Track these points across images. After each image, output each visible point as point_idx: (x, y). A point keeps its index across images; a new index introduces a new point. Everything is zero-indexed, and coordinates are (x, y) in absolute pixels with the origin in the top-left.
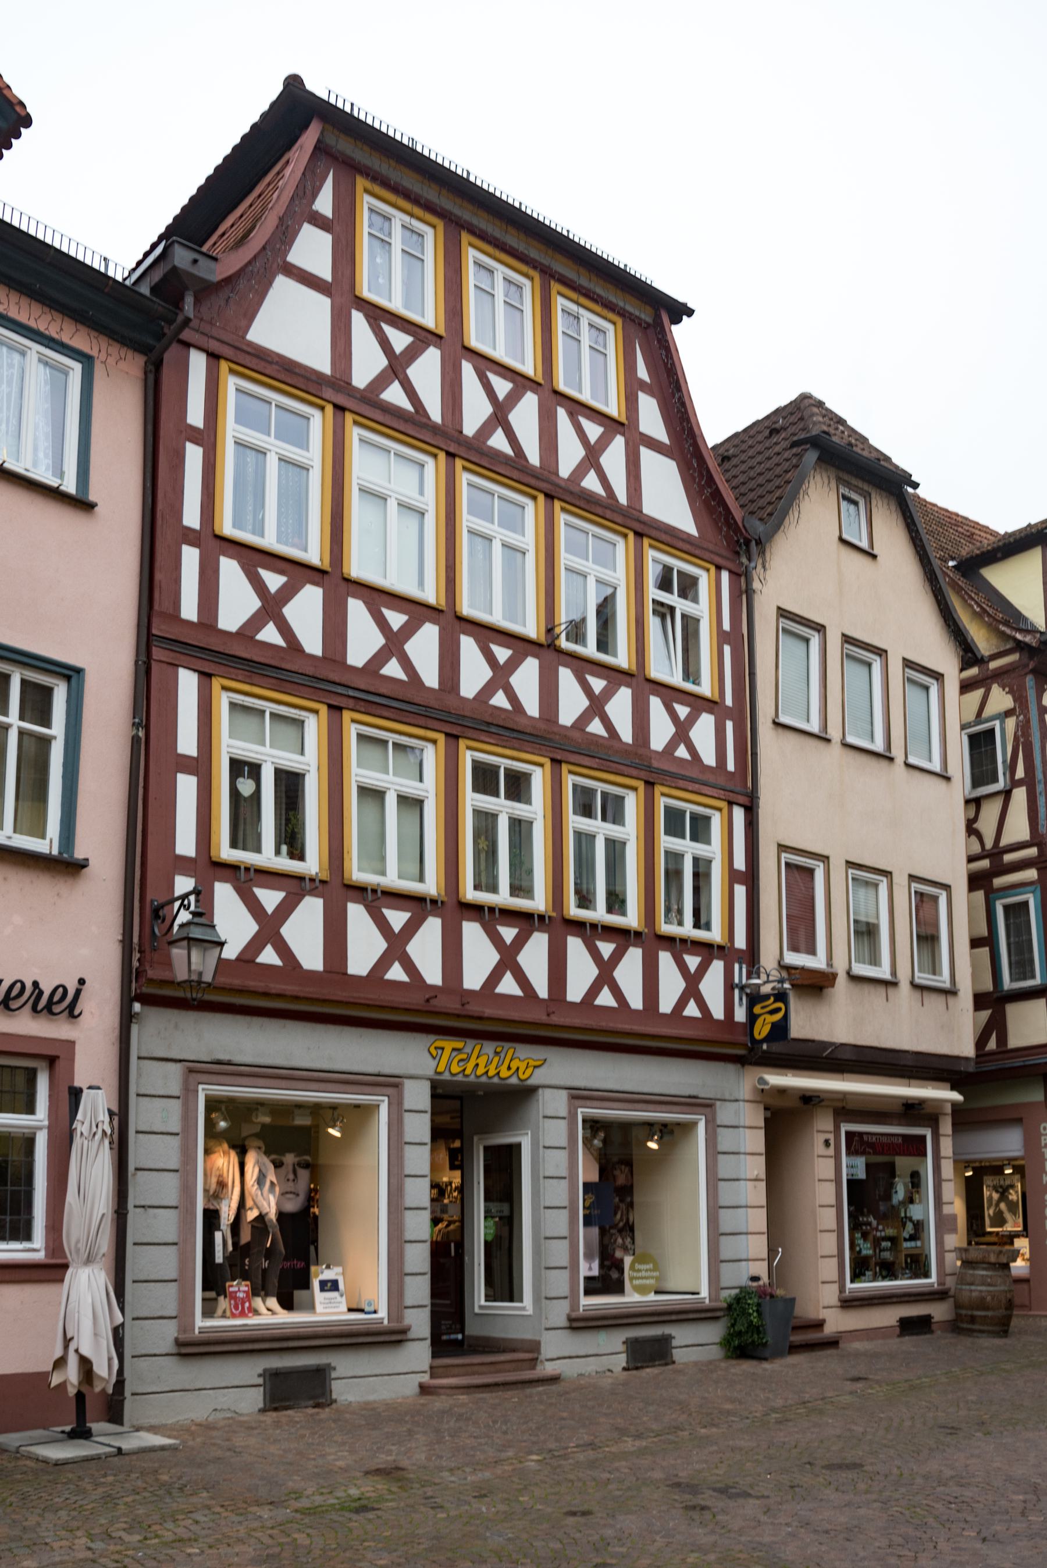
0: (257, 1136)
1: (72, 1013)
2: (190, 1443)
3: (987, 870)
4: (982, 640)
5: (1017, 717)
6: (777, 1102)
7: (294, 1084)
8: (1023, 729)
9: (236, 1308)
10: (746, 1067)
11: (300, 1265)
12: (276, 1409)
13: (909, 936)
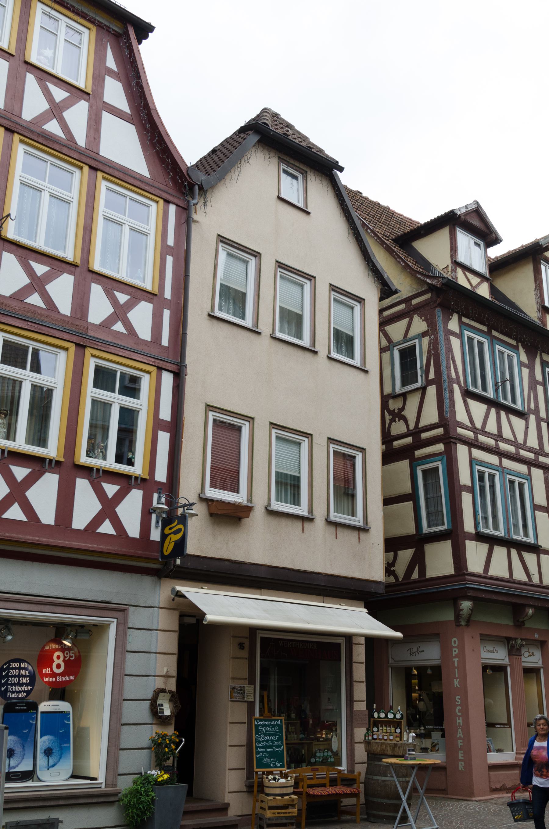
3: (410, 444)
5: (430, 337)
10: (163, 579)
13: (326, 483)
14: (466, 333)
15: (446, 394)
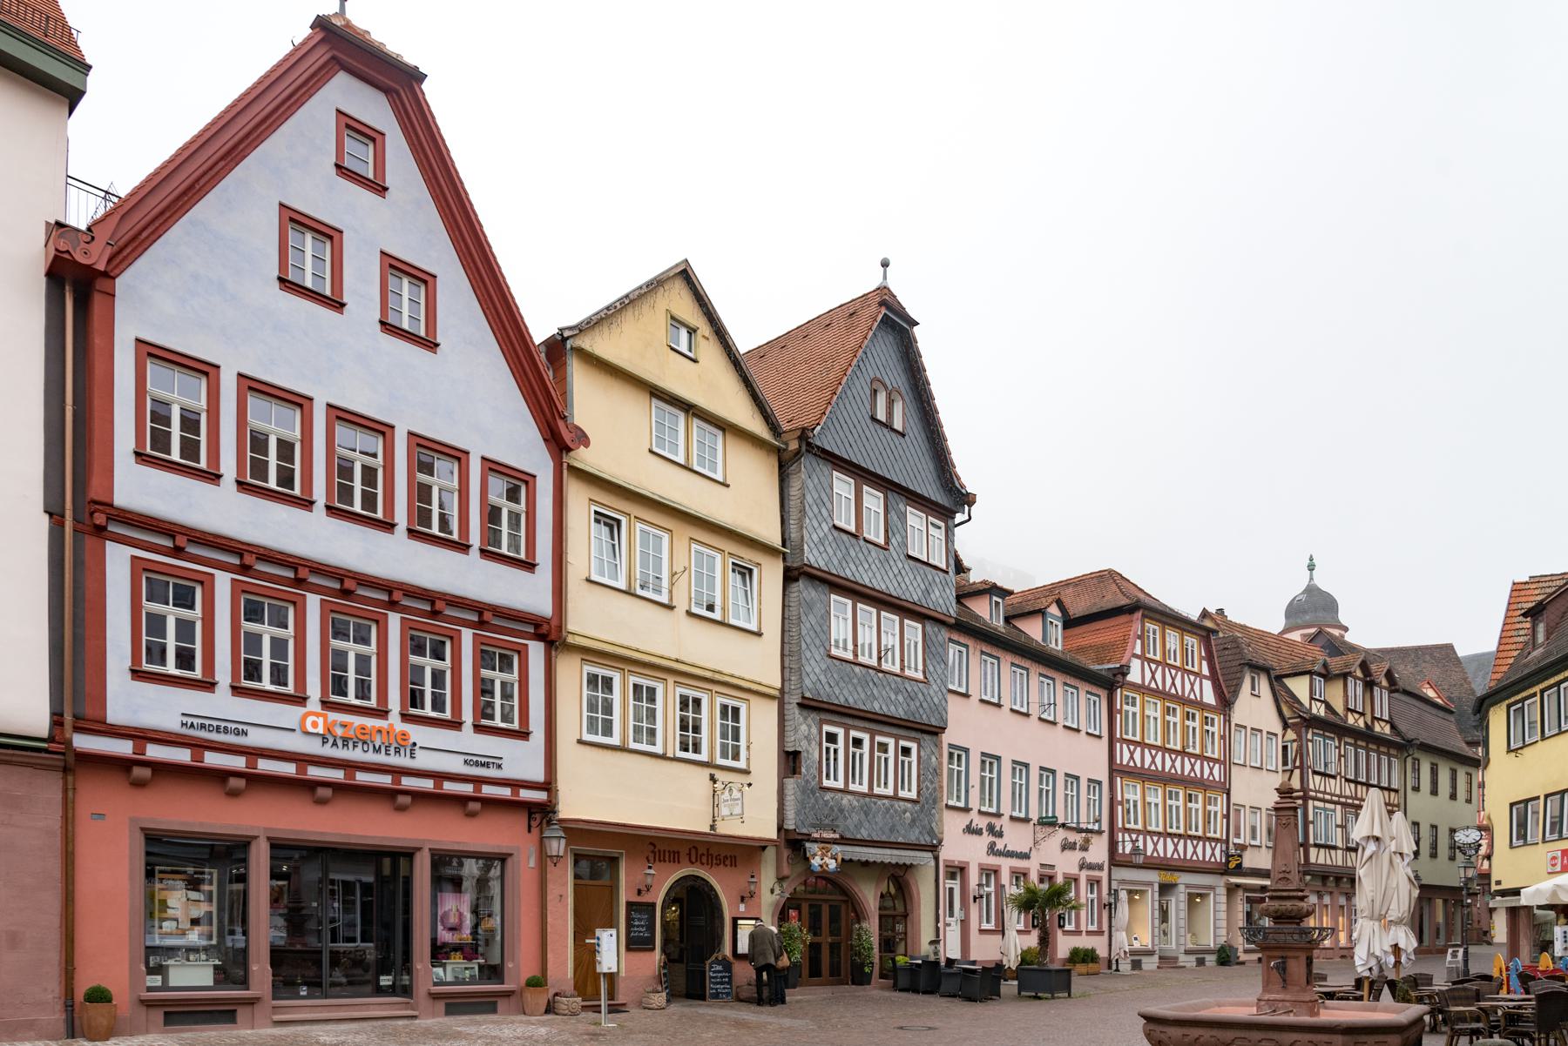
4: (1287, 712)
6: (1230, 887)
8: (1300, 749)
14: (1315, 738)
15: (1305, 775)
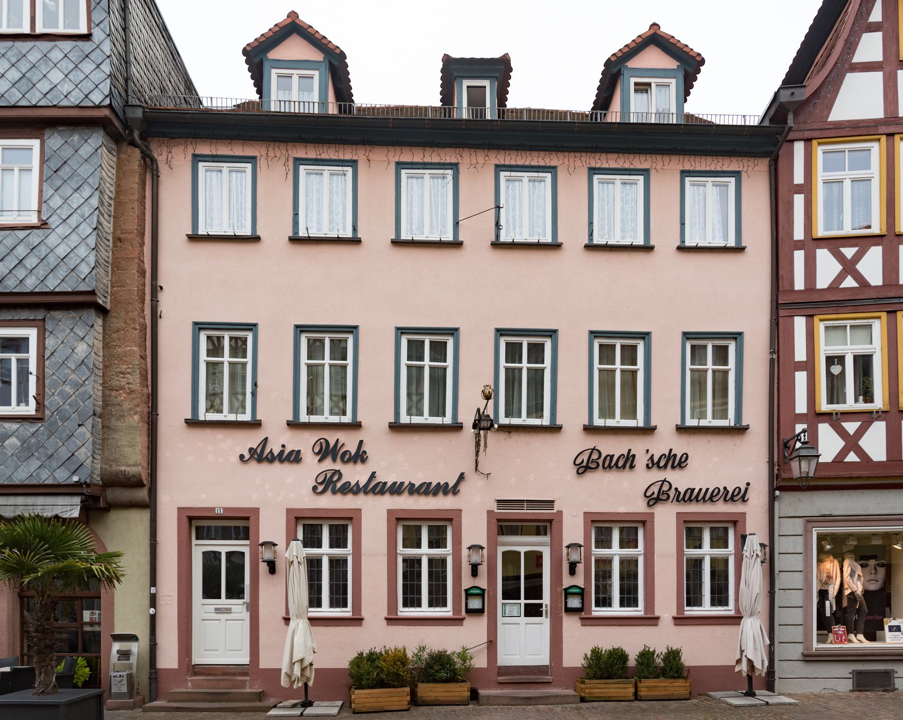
0: (850, 551)
1: (744, 499)
2: (806, 703)
7: (870, 523)
9: (838, 639)
11: (879, 618)
12: (860, 691)
